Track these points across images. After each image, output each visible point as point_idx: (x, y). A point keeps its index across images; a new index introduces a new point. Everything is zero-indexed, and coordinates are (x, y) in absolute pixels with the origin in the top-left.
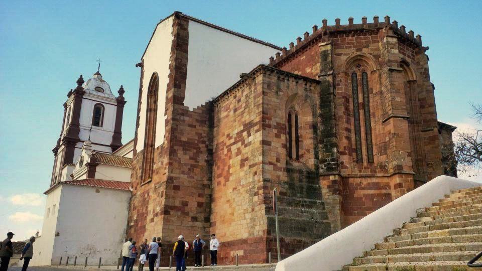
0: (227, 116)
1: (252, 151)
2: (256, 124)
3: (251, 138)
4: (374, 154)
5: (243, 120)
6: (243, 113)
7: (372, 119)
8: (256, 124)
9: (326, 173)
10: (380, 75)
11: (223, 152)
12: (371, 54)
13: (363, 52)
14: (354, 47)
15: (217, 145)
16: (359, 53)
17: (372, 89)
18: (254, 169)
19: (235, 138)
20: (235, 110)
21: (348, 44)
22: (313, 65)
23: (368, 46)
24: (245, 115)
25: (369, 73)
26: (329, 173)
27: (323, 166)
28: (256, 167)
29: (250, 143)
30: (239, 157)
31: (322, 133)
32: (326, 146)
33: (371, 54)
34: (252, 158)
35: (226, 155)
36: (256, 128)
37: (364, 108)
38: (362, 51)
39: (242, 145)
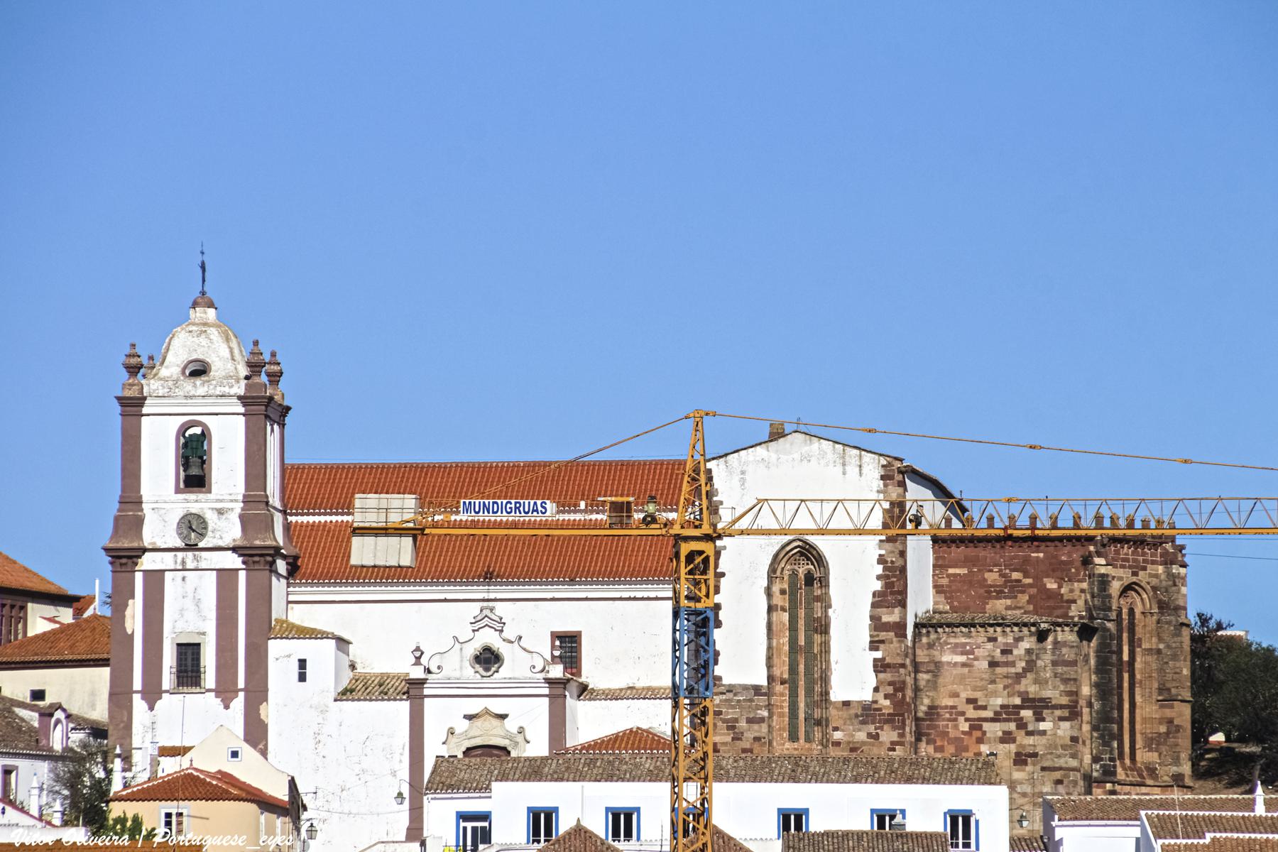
0: (964, 665)
1: (1052, 746)
2: (1061, 707)
3: (1043, 726)
4: (1137, 747)
5: (1022, 688)
6: (1019, 677)
7: (1138, 691)
8: (1056, 707)
9: (1103, 778)
10: (1158, 622)
11: (956, 727)
12: (1148, 583)
13: (1139, 578)
14: (1130, 567)
15: (931, 708)
16: (1134, 579)
17: (1140, 639)
18: (1058, 775)
19: (996, 713)
20: (993, 664)
21: (1124, 560)
22: (1063, 579)
23: (1145, 569)
24: (1024, 681)
25: (1138, 611)
26: (1108, 778)
27: (1098, 767)
28: (1062, 772)
29: (1044, 733)
30: (1012, 748)
31: (1097, 714)
32: (1102, 737)
33: (1148, 583)
34: (1049, 756)
35: (968, 733)
36: (1058, 713)
37: (1129, 671)
38: (1137, 576)
39: (1019, 727)
